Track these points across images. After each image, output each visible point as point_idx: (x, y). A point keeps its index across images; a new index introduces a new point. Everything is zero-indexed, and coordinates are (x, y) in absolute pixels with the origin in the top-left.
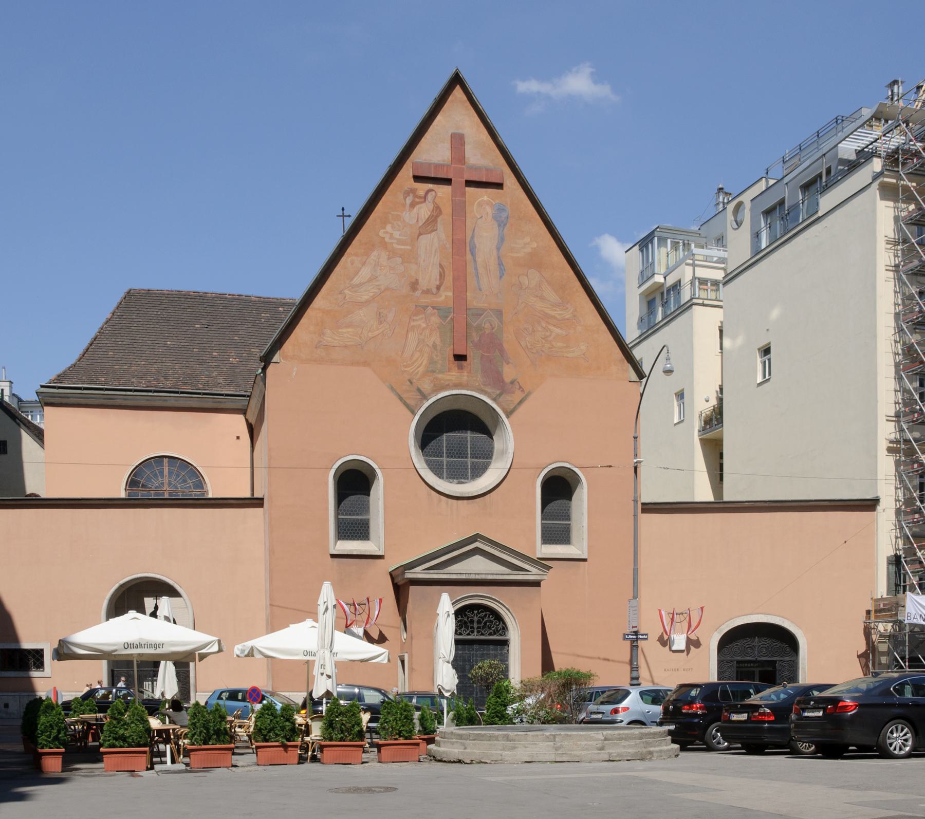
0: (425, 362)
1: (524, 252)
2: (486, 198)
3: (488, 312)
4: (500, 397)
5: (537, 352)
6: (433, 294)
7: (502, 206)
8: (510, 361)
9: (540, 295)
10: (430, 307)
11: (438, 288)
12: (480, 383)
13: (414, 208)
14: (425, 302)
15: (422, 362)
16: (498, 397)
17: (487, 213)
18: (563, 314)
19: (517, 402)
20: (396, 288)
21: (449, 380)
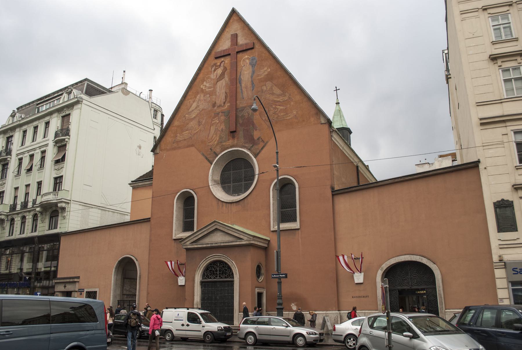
4: (252, 148)
8: (257, 129)
11: (224, 103)
15: (217, 139)
21: (228, 145)
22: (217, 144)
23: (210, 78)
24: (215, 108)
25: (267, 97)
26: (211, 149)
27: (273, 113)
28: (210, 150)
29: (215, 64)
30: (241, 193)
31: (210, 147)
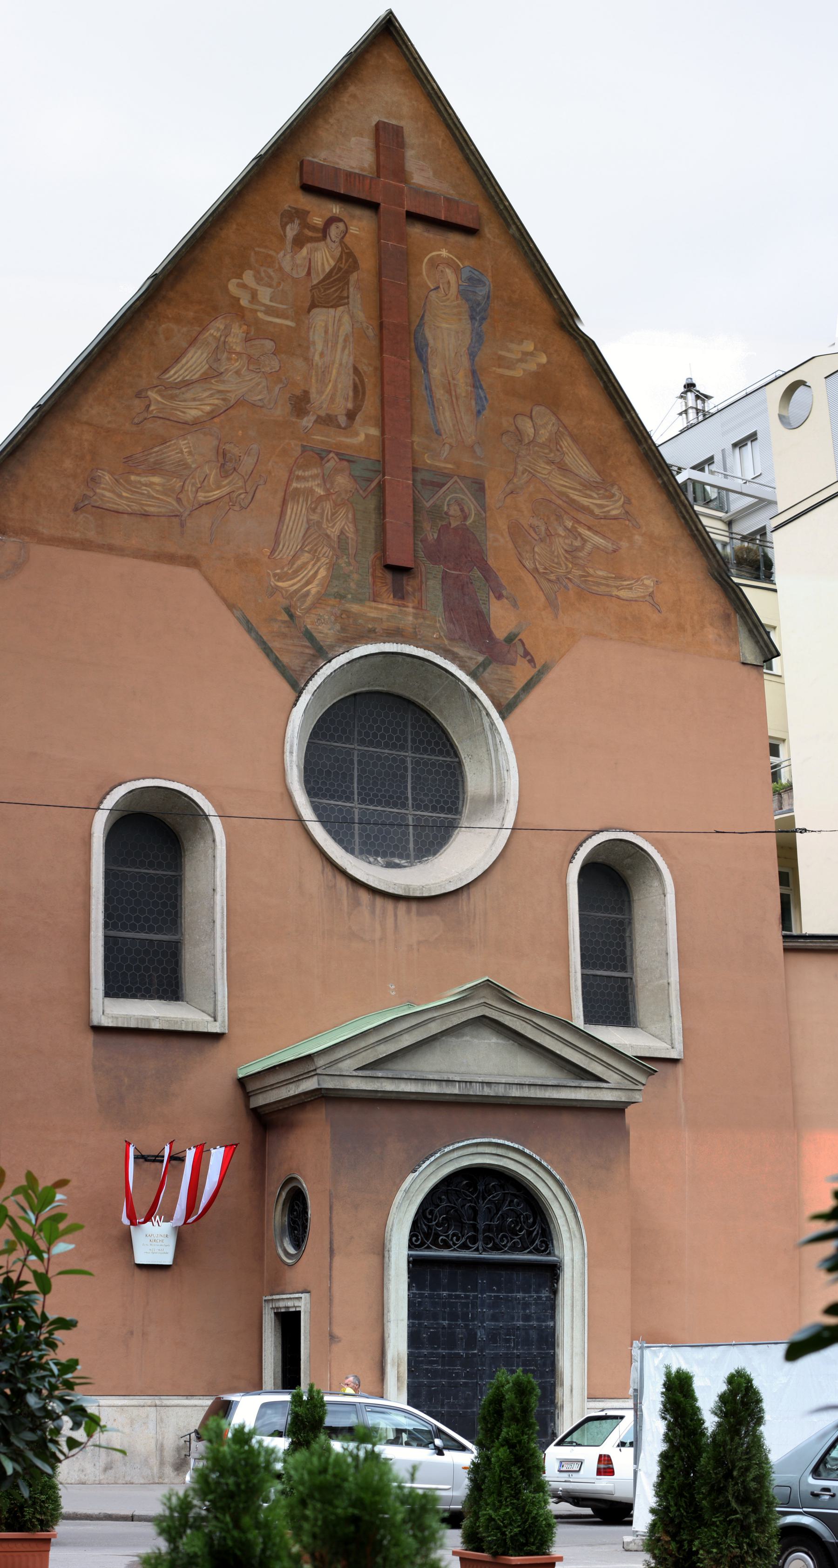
0: (322, 573)
1: (524, 370)
2: (444, 253)
3: (456, 482)
4: (485, 669)
5: (558, 579)
6: (339, 427)
7: (476, 273)
8: (504, 593)
9: (558, 460)
10: (332, 455)
11: (351, 416)
12: (442, 634)
13: (301, 248)
14: (322, 442)
15: (316, 572)
16: (481, 669)
17: (449, 282)
18: (607, 506)
19: (520, 684)
20: (260, 404)
21: (374, 619)
22: (320, 600)
23: (277, 266)
24: (306, 419)
25: (539, 469)
26: (289, 612)
27: (566, 551)
28: (285, 617)
29: (301, 215)
30: (401, 857)
31: (285, 602)
